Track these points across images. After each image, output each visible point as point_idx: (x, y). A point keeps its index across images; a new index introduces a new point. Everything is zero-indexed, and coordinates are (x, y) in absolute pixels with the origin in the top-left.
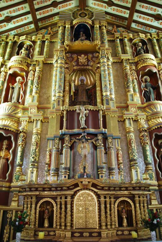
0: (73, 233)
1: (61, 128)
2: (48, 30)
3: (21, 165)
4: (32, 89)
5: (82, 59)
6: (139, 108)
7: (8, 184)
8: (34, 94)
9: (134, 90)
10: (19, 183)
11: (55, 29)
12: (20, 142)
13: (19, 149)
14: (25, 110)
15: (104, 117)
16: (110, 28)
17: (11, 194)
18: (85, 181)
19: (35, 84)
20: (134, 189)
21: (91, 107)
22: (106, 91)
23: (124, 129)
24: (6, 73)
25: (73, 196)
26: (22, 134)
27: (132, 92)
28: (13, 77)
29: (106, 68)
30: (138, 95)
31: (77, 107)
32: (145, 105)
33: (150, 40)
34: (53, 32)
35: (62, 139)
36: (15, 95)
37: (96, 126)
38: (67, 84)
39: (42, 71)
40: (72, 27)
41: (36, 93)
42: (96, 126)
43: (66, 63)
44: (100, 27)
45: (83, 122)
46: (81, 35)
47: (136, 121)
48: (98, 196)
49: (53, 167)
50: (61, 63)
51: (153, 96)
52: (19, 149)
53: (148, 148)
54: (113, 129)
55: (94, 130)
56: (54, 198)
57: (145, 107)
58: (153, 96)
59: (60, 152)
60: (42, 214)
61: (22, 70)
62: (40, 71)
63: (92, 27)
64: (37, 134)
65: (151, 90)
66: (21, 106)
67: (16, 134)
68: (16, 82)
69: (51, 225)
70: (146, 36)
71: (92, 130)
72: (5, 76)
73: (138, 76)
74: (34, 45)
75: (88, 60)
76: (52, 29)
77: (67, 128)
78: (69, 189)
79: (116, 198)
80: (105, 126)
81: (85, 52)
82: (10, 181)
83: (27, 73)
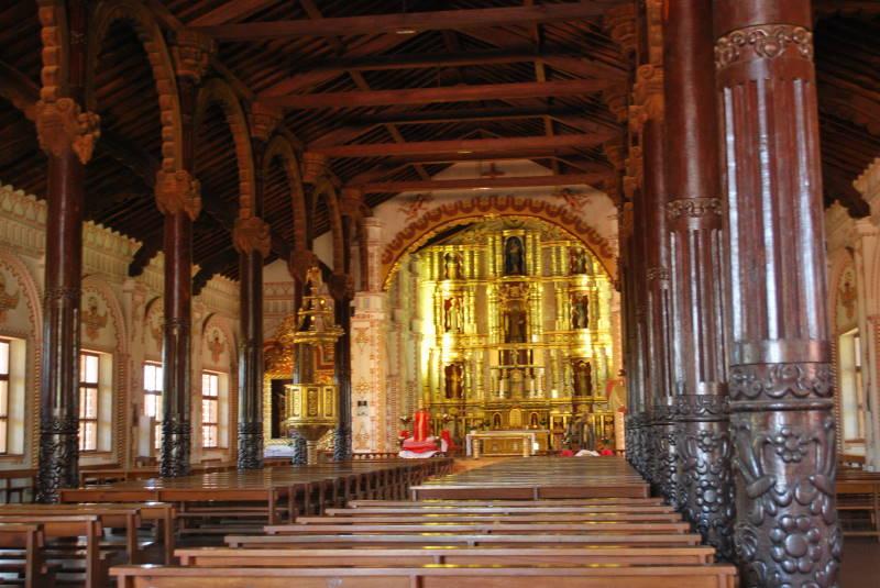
4: (469, 313)
5: (514, 288)
6: (565, 335)
11: (483, 231)
12: (467, 369)
15: (532, 351)
18: (516, 405)
21: (521, 347)
24: (441, 297)
28: (448, 304)
31: (509, 347)
35: (501, 370)
37: (525, 363)
39: (476, 296)
40: (503, 238)
42: (525, 363)
44: (534, 236)
53: (567, 373)
54: (538, 361)
55: (522, 366)
59: (500, 378)
61: (457, 297)
63: (524, 237)
64: (481, 363)
67: (463, 362)
71: (522, 366)
75: (520, 292)
80: (532, 362)
81: (517, 284)
83: (462, 297)
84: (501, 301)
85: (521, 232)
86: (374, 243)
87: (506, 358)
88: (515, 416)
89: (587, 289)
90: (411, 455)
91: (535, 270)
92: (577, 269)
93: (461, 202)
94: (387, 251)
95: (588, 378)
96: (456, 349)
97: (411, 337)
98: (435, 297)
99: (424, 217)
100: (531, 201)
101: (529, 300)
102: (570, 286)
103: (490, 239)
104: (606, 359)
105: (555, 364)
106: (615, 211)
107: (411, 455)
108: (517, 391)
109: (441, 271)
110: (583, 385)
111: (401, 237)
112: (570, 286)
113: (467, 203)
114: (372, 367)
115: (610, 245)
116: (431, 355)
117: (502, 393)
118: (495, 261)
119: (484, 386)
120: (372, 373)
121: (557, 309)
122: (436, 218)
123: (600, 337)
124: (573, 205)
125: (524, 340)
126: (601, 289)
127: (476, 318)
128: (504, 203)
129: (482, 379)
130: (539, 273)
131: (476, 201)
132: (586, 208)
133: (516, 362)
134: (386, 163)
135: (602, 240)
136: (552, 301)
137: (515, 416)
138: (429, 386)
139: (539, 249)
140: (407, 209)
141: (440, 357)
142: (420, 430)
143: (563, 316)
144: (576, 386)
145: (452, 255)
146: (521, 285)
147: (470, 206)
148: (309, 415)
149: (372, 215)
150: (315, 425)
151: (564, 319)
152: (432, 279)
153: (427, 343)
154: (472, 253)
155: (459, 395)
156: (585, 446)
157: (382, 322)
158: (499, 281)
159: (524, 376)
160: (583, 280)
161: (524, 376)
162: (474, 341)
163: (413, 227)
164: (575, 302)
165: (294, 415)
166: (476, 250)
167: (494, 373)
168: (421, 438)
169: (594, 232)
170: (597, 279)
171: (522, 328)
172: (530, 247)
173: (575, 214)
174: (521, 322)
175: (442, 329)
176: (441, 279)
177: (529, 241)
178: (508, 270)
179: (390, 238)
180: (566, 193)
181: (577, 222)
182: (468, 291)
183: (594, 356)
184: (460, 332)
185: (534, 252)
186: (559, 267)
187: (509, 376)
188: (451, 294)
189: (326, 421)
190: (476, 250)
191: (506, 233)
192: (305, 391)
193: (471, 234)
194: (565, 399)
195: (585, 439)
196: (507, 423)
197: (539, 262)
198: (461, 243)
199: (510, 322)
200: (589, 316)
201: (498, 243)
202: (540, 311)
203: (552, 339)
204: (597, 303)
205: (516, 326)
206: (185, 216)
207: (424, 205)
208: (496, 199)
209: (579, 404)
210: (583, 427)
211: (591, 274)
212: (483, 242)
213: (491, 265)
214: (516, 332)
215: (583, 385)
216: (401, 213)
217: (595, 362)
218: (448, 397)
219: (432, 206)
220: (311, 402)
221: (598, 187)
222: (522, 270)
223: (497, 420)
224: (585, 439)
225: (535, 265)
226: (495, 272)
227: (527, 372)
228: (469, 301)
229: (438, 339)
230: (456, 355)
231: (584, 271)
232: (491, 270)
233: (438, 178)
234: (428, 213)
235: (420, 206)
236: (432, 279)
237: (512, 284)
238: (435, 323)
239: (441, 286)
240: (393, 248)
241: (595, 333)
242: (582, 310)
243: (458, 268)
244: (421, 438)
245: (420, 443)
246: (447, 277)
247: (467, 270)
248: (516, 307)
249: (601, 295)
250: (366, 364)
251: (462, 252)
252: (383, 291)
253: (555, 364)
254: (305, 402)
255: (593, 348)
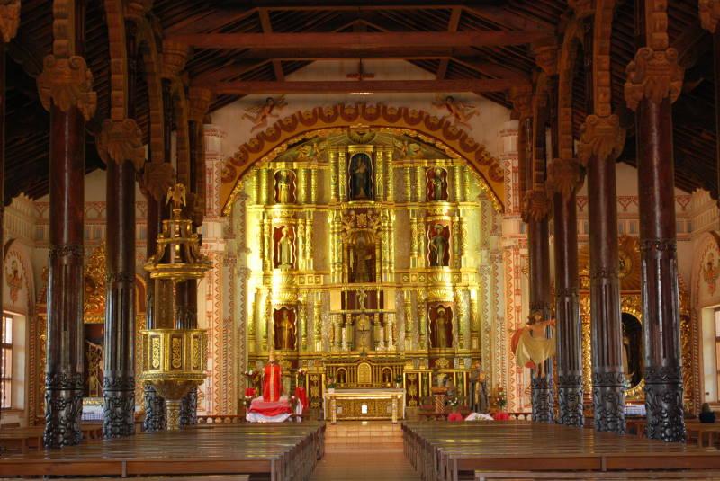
0: (358, 385)
1: (343, 308)
2: (313, 145)
3: (305, 336)
4: (304, 247)
5: (362, 218)
7: (296, 353)
8: (308, 257)
9: (419, 250)
10: (307, 352)
11: (323, 146)
12: (302, 314)
13: (303, 322)
14: (301, 275)
15: (382, 293)
16: (399, 144)
17: (300, 361)
19: (308, 244)
20: (393, 362)
21: (369, 287)
22: (386, 266)
23: (402, 298)
24: (270, 225)
25: (357, 366)
26: (303, 307)
27: (416, 256)
29: (387, 236)
30: (423, 256)
31: (355, 287)
32: (429, 270)
33: (452, 170)
34: (321, 151)
35: (344, 316)
36: (284, 255)
38: (346, 252)
40: (348, 155)
41: (311, 256)
42: (374, 307)
43: (344, 224)
44: (384, 154)
45: (362, 304)
46: (359, 163)
47: (414, 293)
48: (372, 366)
49: (337, 340)
50: (338, 228)
51: (440, 257)
52: (303, 322)
53: (423, 320)
55: (371, 311)
56: (346, 367)
57: (428, 273)
58: (440, 257)
59: (343, 325)
60: (339, 376)
61: (290, 225)
62: (312, 225)
63: (374, 155)
64: (319, 307)
65: (441, 247)
66: (294, 273)
68: (283, 235)
69: (345, 381)
70: (446, 163)
71: (371, 311)
72: (270, 230)
73: (427, 229)
74: (297, 173)
75: (368, 220)
76: (318, 145)
77: (348, 309)
78: (355, 362)
79: (382, 367)
80: (382, 307)
81: (365, 211)
82: (298, 350)
83: (296, 225)
84: (345, 231)
85: (370, 148)
86: (214, 156)
87: (350, 300)
88: (364, 372)
89: (446, 218)
90: (262, 419)
91: (386, 195)
92: (438, 190)
93: (321, 109)
94: (228, 166)
95: (449, 327)
96: (289, 289)
97: (239, 273)
98: (263, 225)
99: (275, 125)
100: (406, 110)
101: (379, 230)
102: (428, 214)
103: (332, 156)
104: (471, 304)
105: (409, 309)
106: (514, 125)
107: (262, 419)
108: (364, 340)
109: (269, 193)
110: (442, 334)
111: (246, 150)
112: (428, 214)
113: (328, 110)
114: (210, 309)
115: (502, 166)
116: (257, 296)
117: (344, 344)
118: (335, 181)
119: (323, 336)
120: (209, 317)
121: (412, 243)
122: (291, 128)
123: (464, 278)
124: (457, 116)
125: (372, 280)
126: (465, 219)
127: (312, 251)
128: (374, 111)
129: (320, 327)
130: (390, 198)
131: (339, 108)
132: (472, 121)
133: (362, 306)
134: (243, 58)
135: (492, 160)
136: (406, 234)
137: (364, 372)
138: (254, 334)
139: (391, 169)
140: (255, 115)
141: (269, 298)
142: (272, 389)
143: (419, 250)
144: (434, 336)
145: (284, 174)
146: (370, 212)
147: (332, 113)
148: (172, 367)
149: (210, 123)
150: (180, 381)
151: (419, 255)
152: (258, 202)
153: (254, 281)
154: (308, 174)
155: (291, 346)
156: (476, 408)
157: (221, 253)
158: (344, 206)
159: (373, 323)
160: (444, 207)
161: (373, 323)
162: (309, 281)
163: (262, 138)
164: (434, 233)
165: (152, 368)
166: (314, 168)
167: (335, 320)
168: (272, 399)
169: (482, 149)
170: (461, 208)
171: (370, 265)
172: (380, 167)
173: (459, 128)
174: (369, 257)
175: (270, 263)
176: (270, 203)
177: (380, 159)
178: (353, 194)
179: (232, 151)
180: (449, 103)
181: (462, 137)
182: (304, 218)
183: (456, 300)
184: (293, 266)
185: (386, 173)
186: (414, 192)
187: (353, 323)
188: (283, 222)
189: (194, 376)
190: (314, 168)
191: (351, 149)
192: (168, 339)
193: (307, 148)
194: (420, 351)
195: (477, 400)
196: (354, 379)
197: (391, 186)
198: (295, 159)
199: (355, 257)
200: (450, 251)
201: (342, 160)
202: (392, 244)
203: (405, 278)
204: (460, 236)
205: (362, 262)
206: (77, 113)
207: (275, 111)
208: (364, 107)
209: (437, 358)
210: (473, 385)
211: (453, 200)
212: (323, 159)
213: (333, 187)
214: (363, 270)
215: (442, 334)
216: (247, 120)
217: (457, 308)
218: (277, 347)
219: (285, 113)
220: (175, 352)
221: (498, 98)
222: (370, 194)
223: (342, 377)
224: (477, 400)
225: (386, 188)
226: (337, 195)
227: (377, 319)
228: (304, 231)
229: (266, 276)
230: (287, 296)
231: (444, 198)
232: (333, 193)
233: (294, 78)
234: (280, 121)
235: (270, 112)
236: (258, 202)
237: (358, 211)
238: (263, 256)
239: (270, 212)
240: (237, 164)
241: (457, 273)
242: (442, 246)
243: (292, 191)
244: (272, 399)
245: (272, 404)
246: (278, 201)
247: (303, 192)
248: (363, 240)
249: (464, 226)
250: (207, 307)
251: (296, 171)
252: (223, 215)
253: (409, 309)
254: (167, 351)
255: (454, 290)
